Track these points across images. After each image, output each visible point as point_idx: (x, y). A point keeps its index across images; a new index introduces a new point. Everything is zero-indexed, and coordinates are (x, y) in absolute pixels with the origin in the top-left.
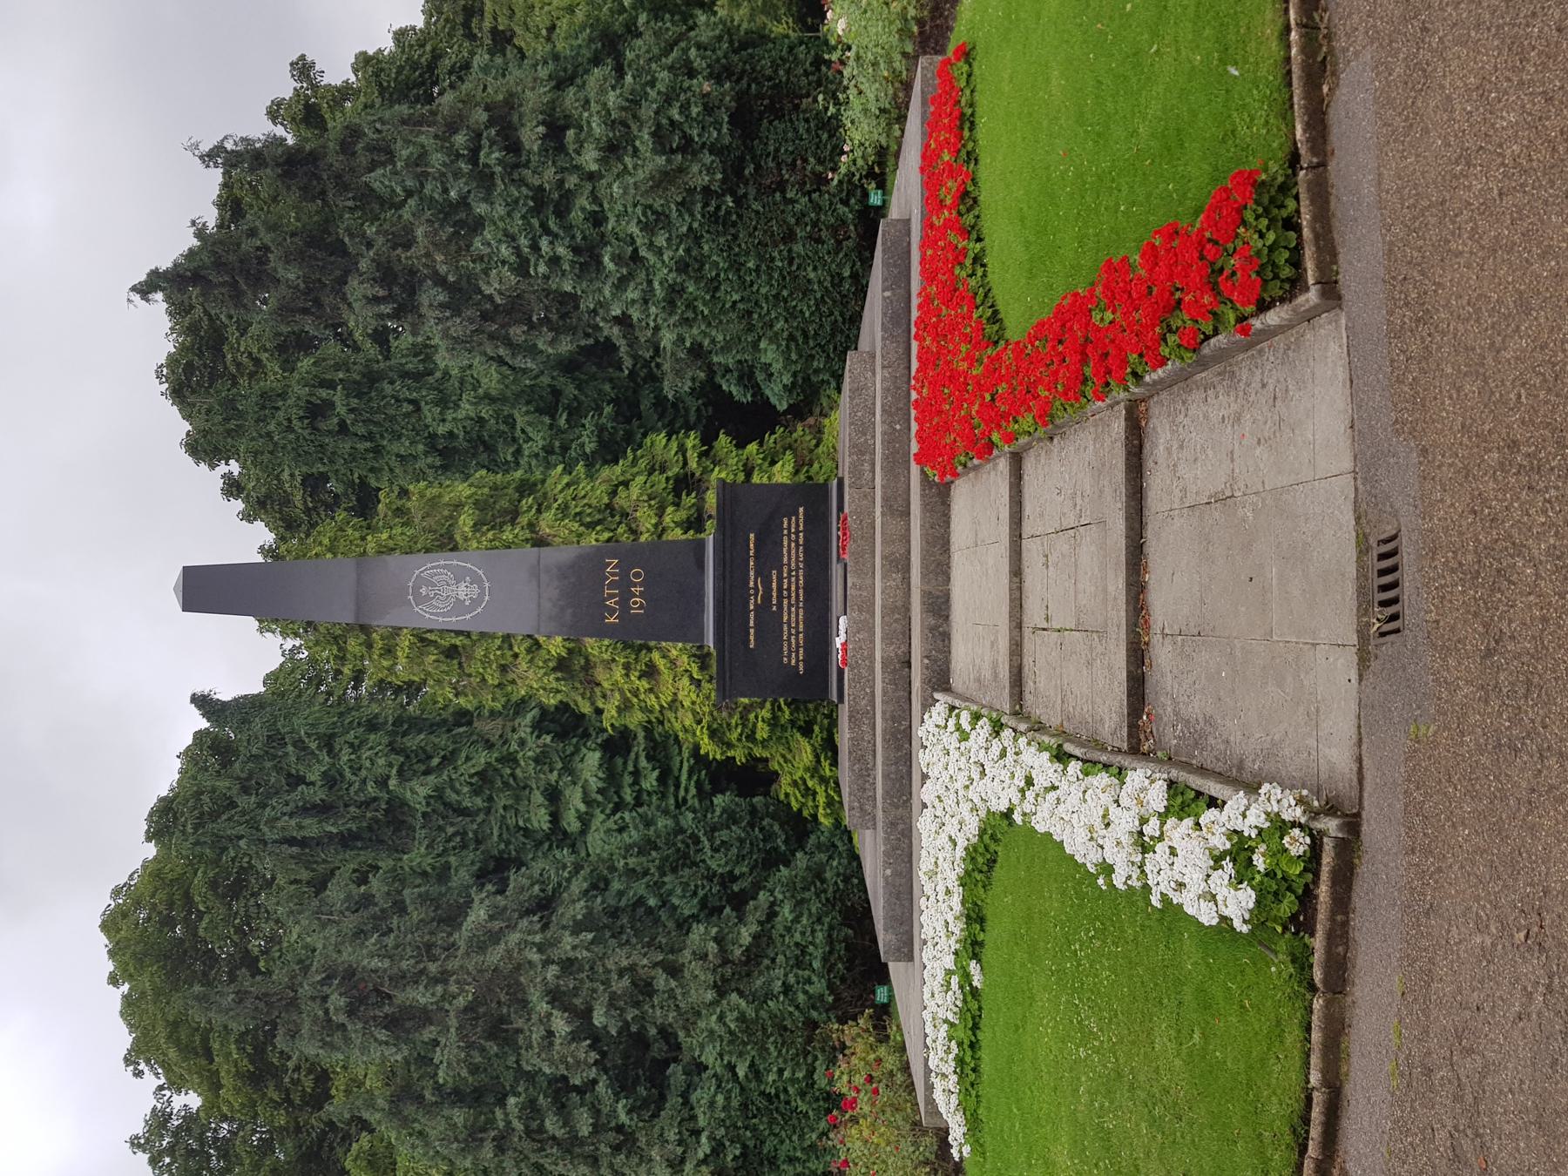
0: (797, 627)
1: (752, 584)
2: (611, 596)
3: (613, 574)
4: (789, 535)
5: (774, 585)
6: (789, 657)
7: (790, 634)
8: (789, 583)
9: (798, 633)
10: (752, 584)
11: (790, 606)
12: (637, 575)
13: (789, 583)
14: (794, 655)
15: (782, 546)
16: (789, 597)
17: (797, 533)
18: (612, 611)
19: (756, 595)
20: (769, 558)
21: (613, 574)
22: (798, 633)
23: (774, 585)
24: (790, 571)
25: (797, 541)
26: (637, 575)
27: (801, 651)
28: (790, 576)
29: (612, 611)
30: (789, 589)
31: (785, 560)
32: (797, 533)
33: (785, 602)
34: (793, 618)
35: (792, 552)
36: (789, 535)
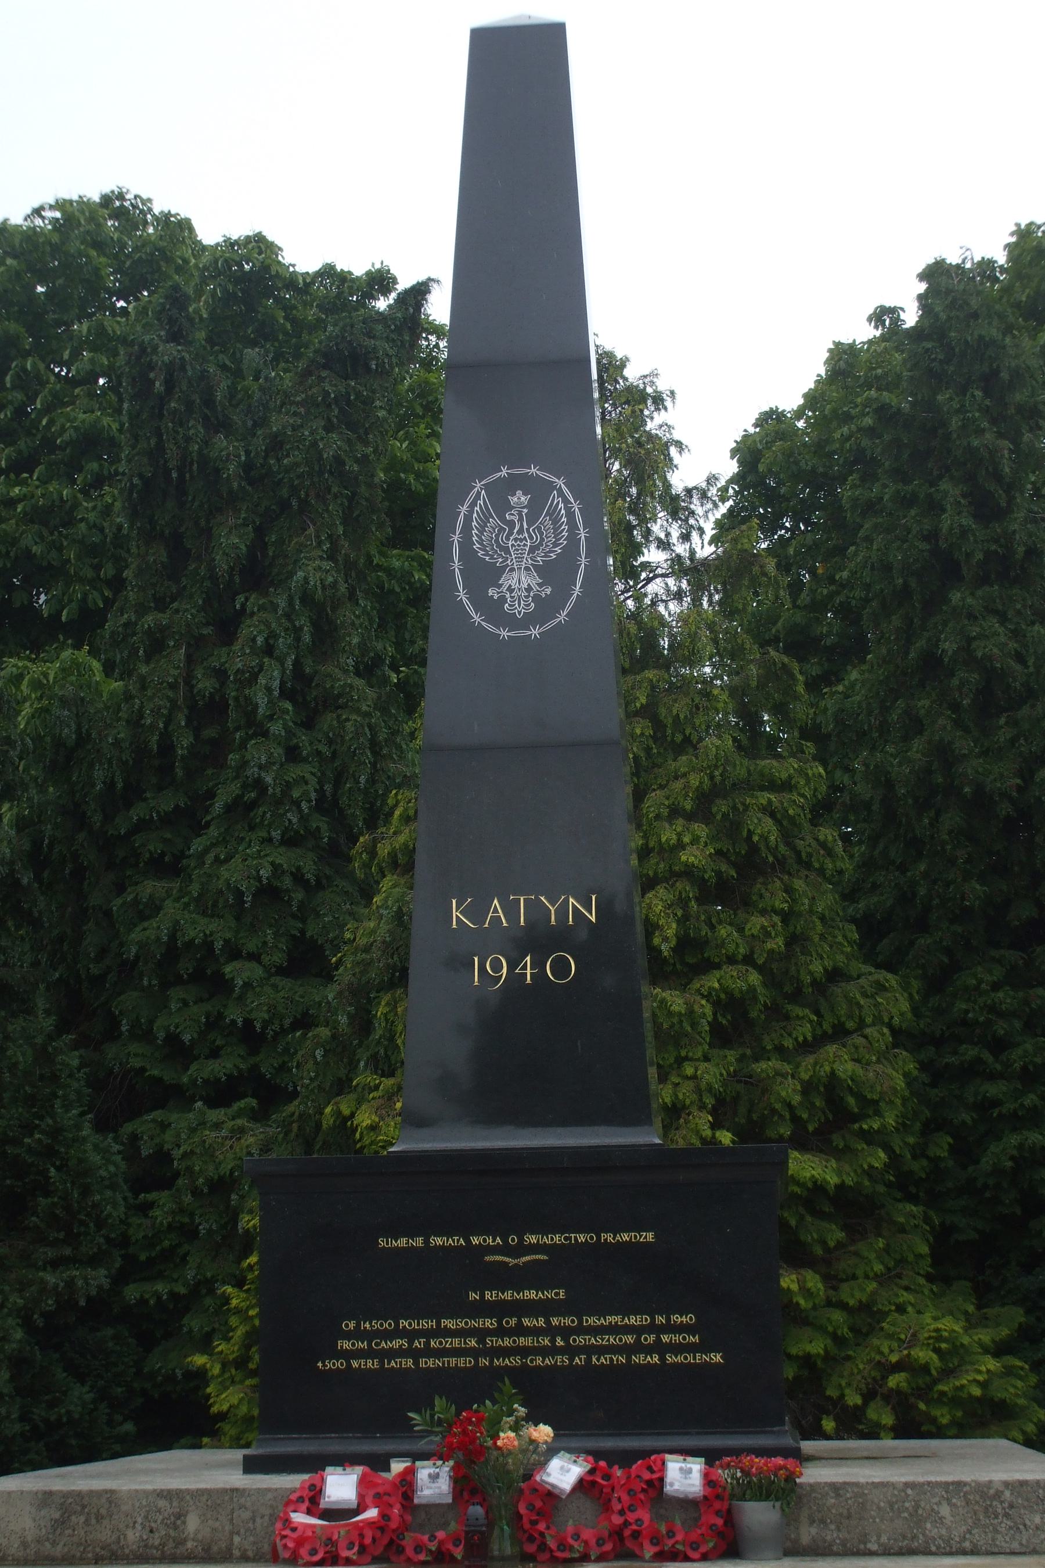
0: (428, 1352)
1: (532, 1239)
2: (511, 909)
3: (563, 911)
4: (652, 1328)
5: (531, 1295)
6: (358, 1334)
7: (411, 1335)
8: (536, 1332)
9: (415, 1354)
10: (532, 1239)
11: (481, 1334)
12: (561, 969)
13: (536, 1332)
14: (365, 1346)
15: (626, 1314)
16: (501, 1332)
17: (660, 1348)
18: (477, 912)
19: (505, 1249)
20: (594, 1280)
21: (563, 911)
22: (415, 1354)
23: (531, 1295)
24: (566, 1332)
25: (638, 1348)
26: (561, 969)
27: (372, 1364)
28: (550, 1331)
29: (477, 912)
30: (521, 1331)
31: (592, 1321)
32: (660, 1348)
33: (490, 1323)
34: (452, 1341)
35: (616, 1337)
36: (652, 1328)
